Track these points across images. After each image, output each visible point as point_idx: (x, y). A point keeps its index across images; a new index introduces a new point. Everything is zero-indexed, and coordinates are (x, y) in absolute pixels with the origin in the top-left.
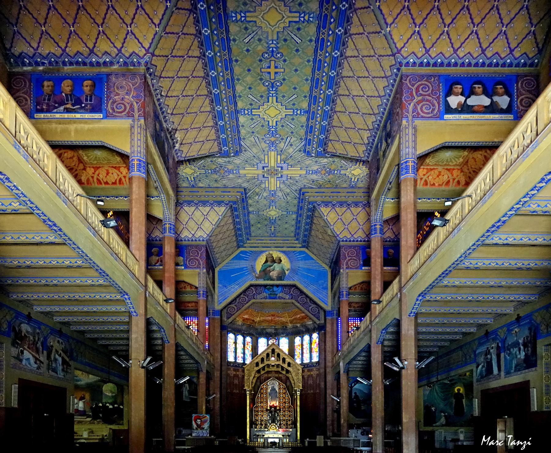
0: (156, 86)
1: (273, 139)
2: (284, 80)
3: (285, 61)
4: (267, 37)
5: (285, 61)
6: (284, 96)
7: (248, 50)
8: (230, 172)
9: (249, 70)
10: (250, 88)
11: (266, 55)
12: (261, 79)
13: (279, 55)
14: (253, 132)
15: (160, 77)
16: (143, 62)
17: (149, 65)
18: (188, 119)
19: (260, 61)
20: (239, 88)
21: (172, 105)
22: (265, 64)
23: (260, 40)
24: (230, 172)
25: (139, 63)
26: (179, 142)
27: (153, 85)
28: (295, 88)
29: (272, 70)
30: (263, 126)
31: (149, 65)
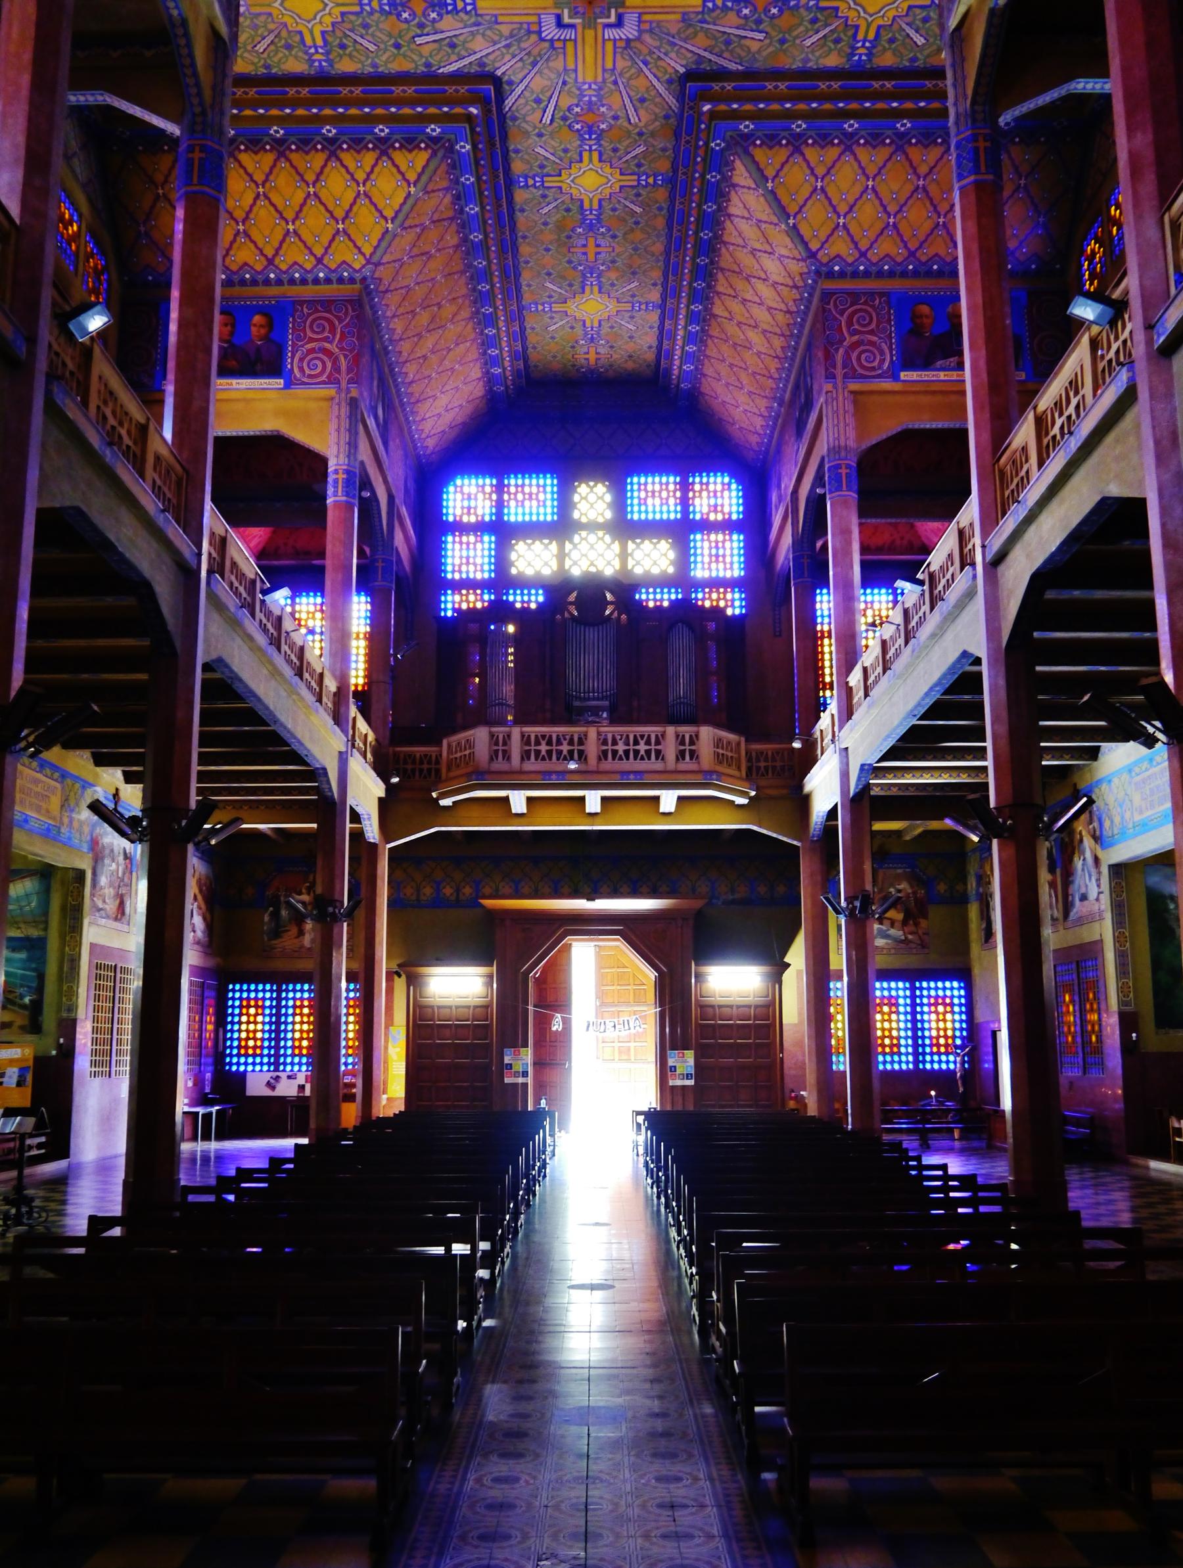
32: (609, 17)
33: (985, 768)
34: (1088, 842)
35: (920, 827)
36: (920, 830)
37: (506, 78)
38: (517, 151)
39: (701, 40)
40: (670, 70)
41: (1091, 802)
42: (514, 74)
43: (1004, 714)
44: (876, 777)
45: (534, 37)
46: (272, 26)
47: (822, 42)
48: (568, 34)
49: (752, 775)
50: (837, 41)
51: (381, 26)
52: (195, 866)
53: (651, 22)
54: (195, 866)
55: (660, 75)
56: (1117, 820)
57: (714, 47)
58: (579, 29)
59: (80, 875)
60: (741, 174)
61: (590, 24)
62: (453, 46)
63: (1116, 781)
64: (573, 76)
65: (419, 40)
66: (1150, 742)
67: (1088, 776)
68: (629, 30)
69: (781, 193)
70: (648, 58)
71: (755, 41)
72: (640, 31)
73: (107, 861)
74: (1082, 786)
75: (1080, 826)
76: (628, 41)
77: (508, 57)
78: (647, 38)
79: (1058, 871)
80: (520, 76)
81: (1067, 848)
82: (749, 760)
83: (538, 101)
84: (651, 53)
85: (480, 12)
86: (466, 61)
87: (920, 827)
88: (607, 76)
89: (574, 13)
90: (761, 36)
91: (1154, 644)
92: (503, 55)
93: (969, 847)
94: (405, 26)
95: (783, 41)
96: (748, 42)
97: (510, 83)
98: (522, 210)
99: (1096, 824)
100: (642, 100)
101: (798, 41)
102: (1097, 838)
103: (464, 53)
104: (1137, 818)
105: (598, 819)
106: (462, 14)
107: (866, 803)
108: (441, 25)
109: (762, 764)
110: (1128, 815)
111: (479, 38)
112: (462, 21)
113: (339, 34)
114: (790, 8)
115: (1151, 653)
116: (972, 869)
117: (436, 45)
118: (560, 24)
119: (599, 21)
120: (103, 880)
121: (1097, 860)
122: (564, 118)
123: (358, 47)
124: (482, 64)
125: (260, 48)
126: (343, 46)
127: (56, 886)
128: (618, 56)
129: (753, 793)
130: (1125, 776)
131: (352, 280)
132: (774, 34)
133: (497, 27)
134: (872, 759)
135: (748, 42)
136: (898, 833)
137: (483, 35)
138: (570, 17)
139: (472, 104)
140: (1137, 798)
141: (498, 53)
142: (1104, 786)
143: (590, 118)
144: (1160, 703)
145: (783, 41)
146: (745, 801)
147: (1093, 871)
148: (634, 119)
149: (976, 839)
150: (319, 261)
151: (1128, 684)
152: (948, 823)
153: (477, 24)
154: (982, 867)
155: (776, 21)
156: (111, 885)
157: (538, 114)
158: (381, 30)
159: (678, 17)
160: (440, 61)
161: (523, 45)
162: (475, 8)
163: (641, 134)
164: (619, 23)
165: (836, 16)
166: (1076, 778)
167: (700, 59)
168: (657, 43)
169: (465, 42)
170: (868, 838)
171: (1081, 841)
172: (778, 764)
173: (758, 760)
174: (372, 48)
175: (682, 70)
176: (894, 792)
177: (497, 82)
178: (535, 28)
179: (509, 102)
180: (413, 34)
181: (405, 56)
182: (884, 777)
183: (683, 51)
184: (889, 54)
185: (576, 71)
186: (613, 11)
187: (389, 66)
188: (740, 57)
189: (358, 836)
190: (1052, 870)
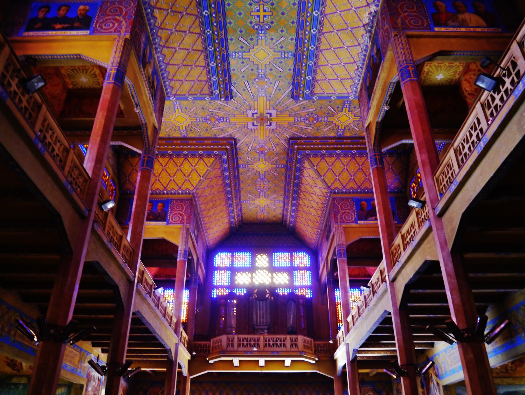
2: (251, 4)
4: (266, 41)
5: (251, 23)
9: (283, 14)
11: (267, 27)
12: (272, 4)
13: (256, 27)
19: (272, 22)
22: (268, 19)
23: (272, 39)
27: (359, 81)
29: (262, 13)
33: (395, 351)
34: (434, 377)
35: (375, 371)
36: (374, 373)
38: (240, 158)
41: (433, 363)
43: (400, 332)
44: (359, 353)
45: (246, 128)
49: (316, 353)
50: (333, 129)
52: (123, 383)
54: (123, 383)
56: (443, 369)
59: (82, 386)
60: (307, 164)
61: (262, 125)
62: (222, 130)
63: (441, 354)
66: (451, 342)
67: (431, 353)
69: (319, 170)
71: (309, 130)
73: (92, 381)
74: (430, 356)
75: (431, 371)
76: (273, 129)
78: (278, 128)
79: (425, 388)
81: (427, 379)
82: (315, 347)
83: (247, 145)
84: (279, 132)
86: (226, 134)
87: (375, 371)
89: (258, 122)
91: (448, 308)
93: (393, 379)
95: (318, 130)
97: (239, 140)
98: (242, 174)
99: (436, 370)
100: (277, 145)
102: (437, 376)
104: (450, 368)
105: (263, 368)
107: (356, 363)
109: (320, 349)
110: (447, 367)
113: (190, 127)
115: (447, 310)
116: (395, 387)
118: (253, 125)
120: (90, 389)
121: (438, 384)
122: (254, 149)
124: (230, 135)
125: (167, 130)
126: (191, 130)
127: (73, 390)
129: (317, 359)
130: (444, 353)
131: (189, 193)
134: (357, 347)
136: (367, 374)
139: (227, 145)
140: (449, 361)
142: (437, 356)
143: (262, 149)
144: (452, 328)
145: (318, 130)
146: (313, 362)
147: (437, 388)
148: (275, 150)
149: (395, 377)
150: (180, 188)
151: (441, 321)
152: (385, 370)
154: (398, 386)
156: (92, 390)
157: (247, 148)
163: (277, 154)
166: (427, 353)
167: (294, 134)
170: (357, 376)
171: (432, 377)
172: (325, 349)
173: (318, 347)
174: (199, 130)
175: (289, 137)
176: (365, 359)
177: (235, 140)
179: (238, 146)
182: (361, 353)
189: (180, 373)
190: (422, 387)
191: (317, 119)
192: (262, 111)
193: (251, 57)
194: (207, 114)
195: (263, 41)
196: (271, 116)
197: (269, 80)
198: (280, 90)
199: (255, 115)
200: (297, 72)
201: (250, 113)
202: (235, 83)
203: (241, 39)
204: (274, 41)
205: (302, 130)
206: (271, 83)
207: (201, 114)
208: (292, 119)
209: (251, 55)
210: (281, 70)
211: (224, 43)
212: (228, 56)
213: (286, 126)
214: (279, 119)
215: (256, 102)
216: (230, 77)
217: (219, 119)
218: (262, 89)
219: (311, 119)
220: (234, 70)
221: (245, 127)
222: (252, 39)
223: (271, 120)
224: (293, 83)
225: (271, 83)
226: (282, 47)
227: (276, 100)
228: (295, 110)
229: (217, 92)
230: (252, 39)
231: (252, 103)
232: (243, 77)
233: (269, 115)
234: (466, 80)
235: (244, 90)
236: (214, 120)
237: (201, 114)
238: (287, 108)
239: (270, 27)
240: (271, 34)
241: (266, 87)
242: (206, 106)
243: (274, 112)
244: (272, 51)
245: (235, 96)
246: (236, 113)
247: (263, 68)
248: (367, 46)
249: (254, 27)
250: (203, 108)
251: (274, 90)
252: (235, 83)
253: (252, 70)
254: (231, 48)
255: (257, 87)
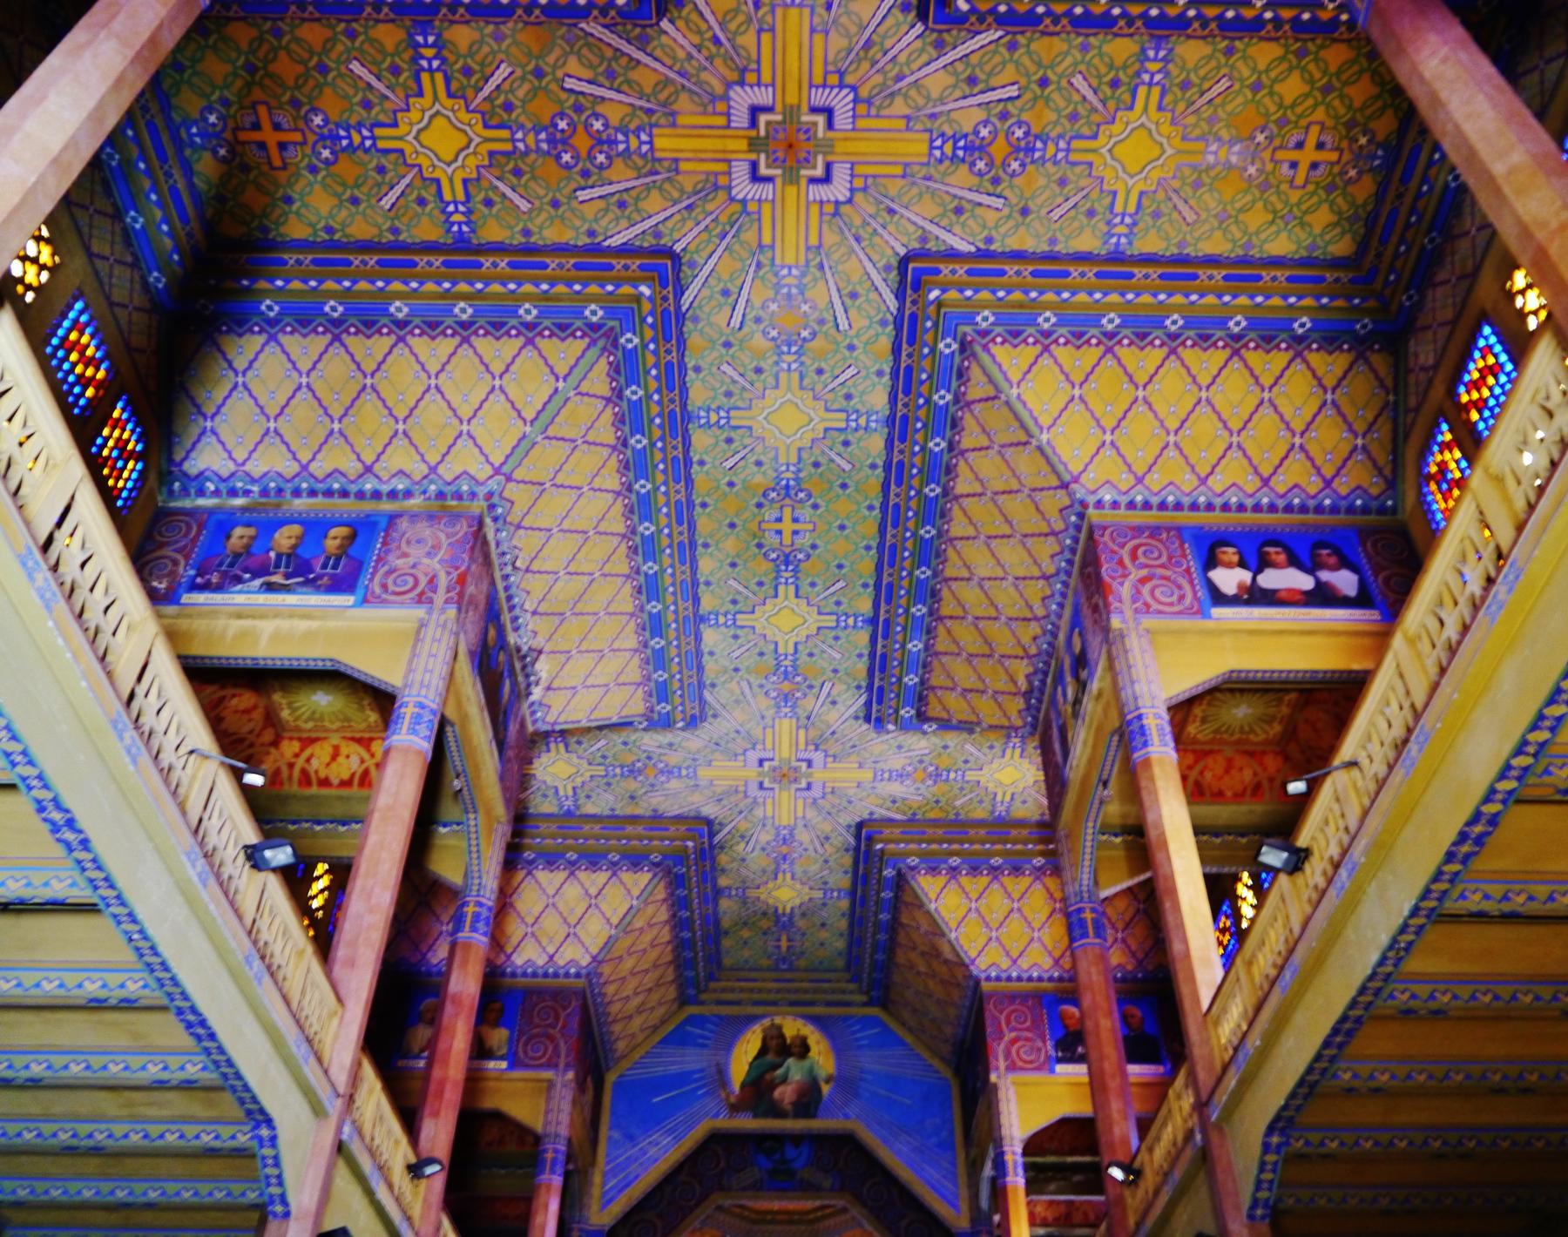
0: (504, 547)
1: (786, 686)
2: (814, 547)
3: (815, 507)
5: (815, 507)
6: (813, 585)
7: (731, 484)
8: (669, 772)
9: (732, 525)
10: (733, 565)
12: (760, 546)
14: (736, 670)
15: (519, 527)
16: (482, 491)
17: (495, 500)
18: (573, 628)
19: (759, 505)
20: (706, 565)
21: (538, 593)
22: (769, 513)
23: (759, 464)
24: (669, 772)
25: (473, 495)
26: (543, 684)
27: (498, 544)
28: (840, 567)
29: (787, 526)
30: (761, 654)
31: (495, 500)
32: (768, 123)
37: (912, 16)
39: (646, 79)
40: (680, 23)
42: (898, 25)
45: (864, 92)
46: (1191, 120)
47: (488, 70)
48: (820, 98)
51: (1053, 116)
53: (715, 113)
55: (694, 17)
57: (627, 68)
58: (805, 108)
61: (791, 112)
62: (972, 81)
64: (816, 20)
65: (1012, 91)
68: (742, 99)
70: (714, 49)
71: (575, 74)
72: (726, 98)
76: (742, 83)
77: (902, 58)
78: (718, 88)
80: (890, 21)
84: (710, 59)
85: (926, 136)
88: (769, 19)
89: (809, 130)
90: (570, 83)
92: (908, 64)
94: (1025, 117)
96: (587, 74)
101: (519, 72)
103: (959, 66)
106: (949, 133)
108: (980, 115)
111: (935, 94)
112: (950, 121)
114: (545, 129)
117: (994, 82)
118: (829, 112)
119: (779, 118)
123: (1095, 82)
124: (939, 45)
128: (754, 56)
132: (554, 87)
133: (907, 111)
135: (587, 74)
137: (928, 98)
138: (815, 124)
141: (914, 66)
153: (933, 116)
155: (556, 109)
158: (1057, 110)
159: (681, 120)
160: (995, 52)
161: (878, 79)
162: (932, 141)
164: (755, 111)
165: (483, 114)
167: (642, 43)
168: (704, 76)
169: (955, 86)
174: (1078, 81)
175: (665, 24)
177: (922, 16)
178: (862, 109)
180: (1018, 103)
181: (1039, 65)
183: (668, 62)
184: (389, 45)
185: (813, 30)
186: (762, 133)
187: (1065, 47)
188: (588, 45)
191: (559, 142)
192: (791, 191)
193: (822, 412)
194: (1017, 181)
195: (782, 459)
196: (754, 166)
197: (765, 333)
198: (726, 293)
199: (819, 172)
200: (675, 377)
201: (838, 189)
202: (883, 323)
203: (848, 467)
204: (752, 459)
205: (611, 75)
206: (758, 320)
207: (1036, 183)
208: (666, 143)
209: (821, 420)
210: (725, 367)
211: (894, 472)
212: (890, 421)
213: (683, 103)
214: (718, 144)
215: (814, 241)
216: (896, 351)
217: (973, 148)
218: (789, 295)
219: (582, 142)
220: (880, 373)
221: (869, 102)
222: (816, 465)
223: (754, 144)
224: (681, 317)
225: (758, 320)
226: (729, 441)
227: (737, 247)
228: (655, 194)
229: (948, 346)
230: (816, 465)
231: (830, 238)
232: (851, 348)
233: (764, 171)
234: (255, 707)
235: (854, 295)
236: (992, 149)
237: (1042, 181)
238: (689, 207)
239: (765, 495)
240: (762, 478)
241: (774, 307)
242: (1011, 223)
243: (743, 187)
244: (757, 432)
245: (888, 268)
246: (894, 187)
247: (783, 376)
248: (516, 629)
249: (810, 496)
250: (1025, 212)
251: (745, 293)
252: (883, 323)
253: (820, 372)
254: (875, 444)
255: (805, 308)
